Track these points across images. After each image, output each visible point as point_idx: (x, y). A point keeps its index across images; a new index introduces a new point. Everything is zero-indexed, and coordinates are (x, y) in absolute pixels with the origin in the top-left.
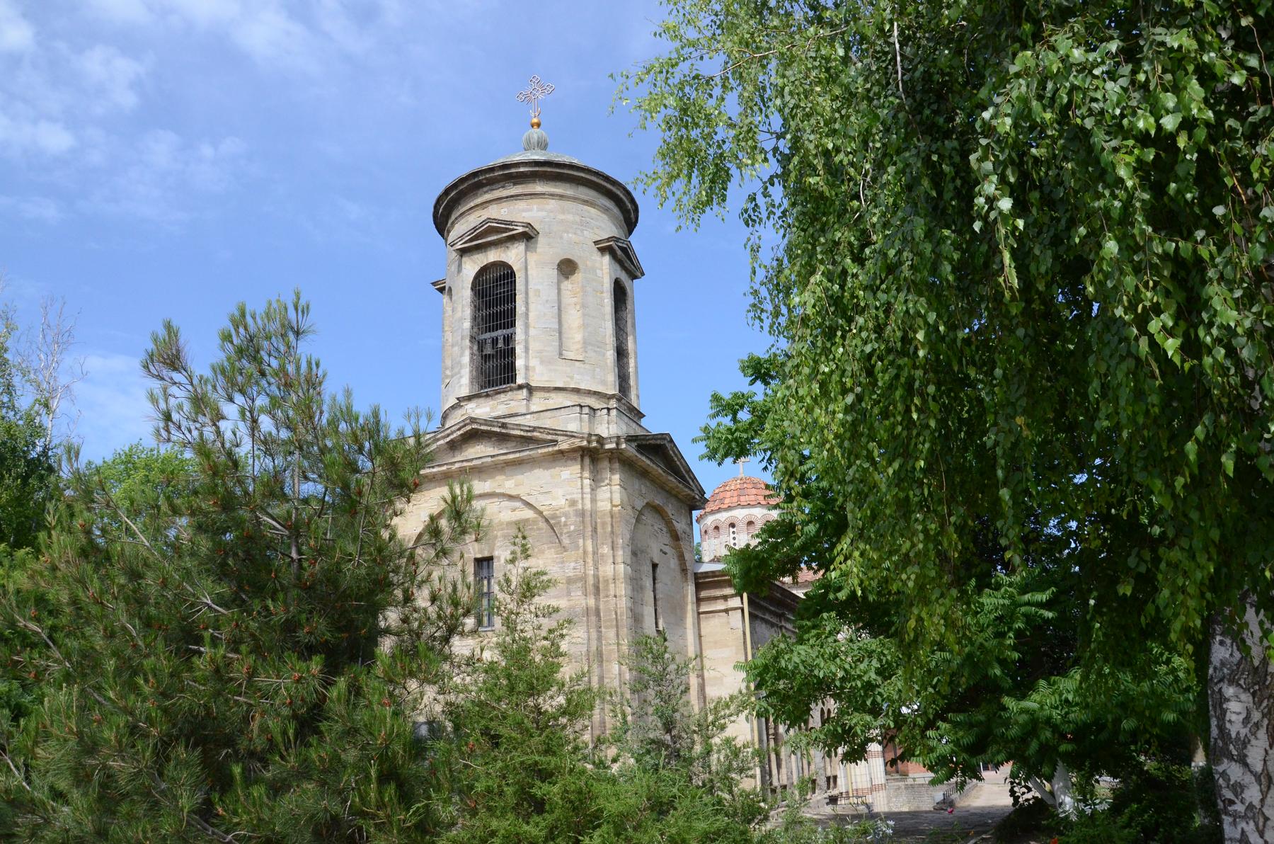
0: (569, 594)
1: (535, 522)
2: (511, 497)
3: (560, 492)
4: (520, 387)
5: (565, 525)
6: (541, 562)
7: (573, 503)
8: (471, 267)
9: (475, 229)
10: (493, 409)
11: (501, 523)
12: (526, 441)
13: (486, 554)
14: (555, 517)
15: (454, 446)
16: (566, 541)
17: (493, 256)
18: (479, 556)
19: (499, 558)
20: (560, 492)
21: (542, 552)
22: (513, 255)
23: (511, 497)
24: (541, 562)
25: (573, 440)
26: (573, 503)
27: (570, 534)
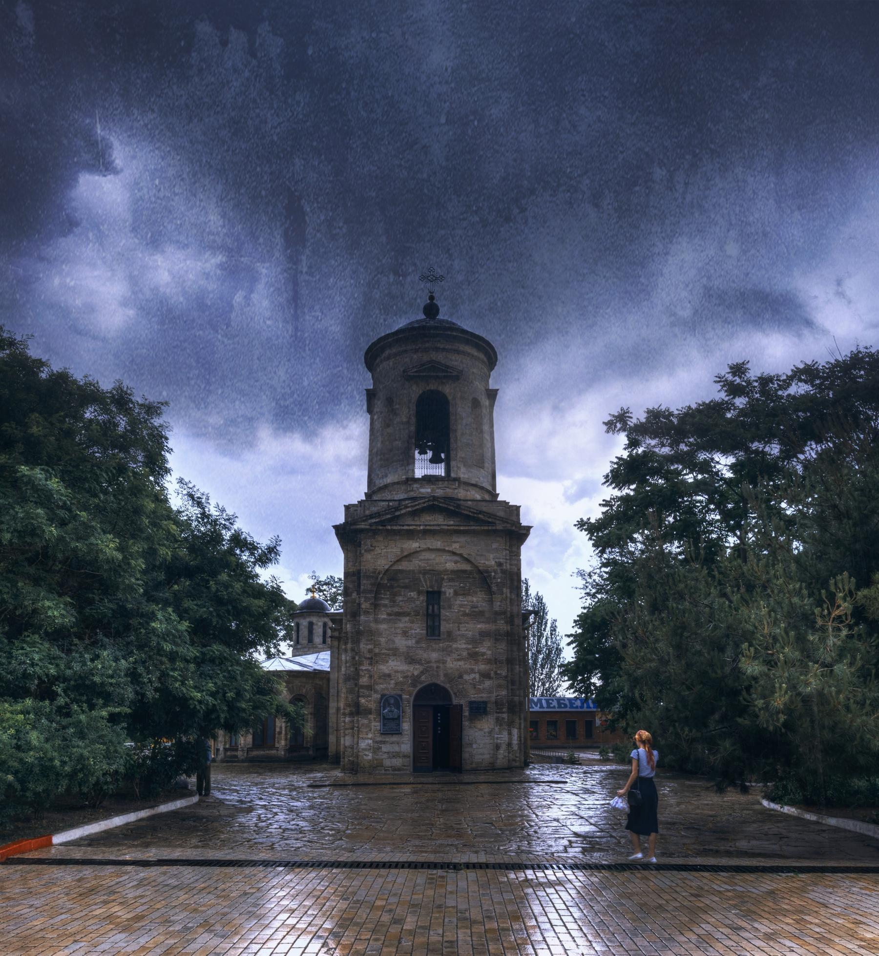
0: (495, 622)
1: (471, 572)
2: (454, 553)
3: (492, 556)
4: (455, 480)
5: (494, 578)
6: (475, 599)
7: (500, 564)
8: (415, 391)
9: (422, 365)
10: (433, 490)
11: (446, 571)
12: (467, 518)
13: (436, 589)
14: (487, 571)
15: (415, 514)
16: (494, 588)
17: (433, 386)
18: (430, 589)
19: (445, 593)
20: (492, 556)
21: (476, 593)
22: (447, 389)
23: (454, 553)
24: (475, 599)
25: (505, 525)
26: (500, 564)
27: (497, 584)
